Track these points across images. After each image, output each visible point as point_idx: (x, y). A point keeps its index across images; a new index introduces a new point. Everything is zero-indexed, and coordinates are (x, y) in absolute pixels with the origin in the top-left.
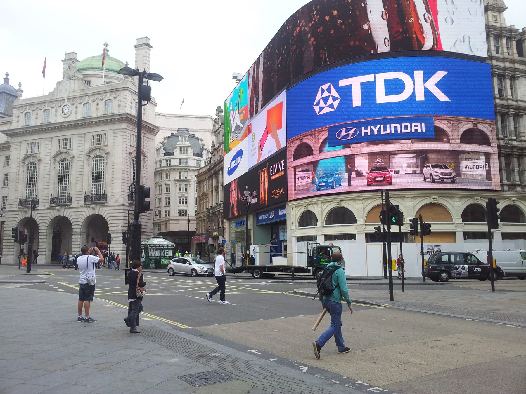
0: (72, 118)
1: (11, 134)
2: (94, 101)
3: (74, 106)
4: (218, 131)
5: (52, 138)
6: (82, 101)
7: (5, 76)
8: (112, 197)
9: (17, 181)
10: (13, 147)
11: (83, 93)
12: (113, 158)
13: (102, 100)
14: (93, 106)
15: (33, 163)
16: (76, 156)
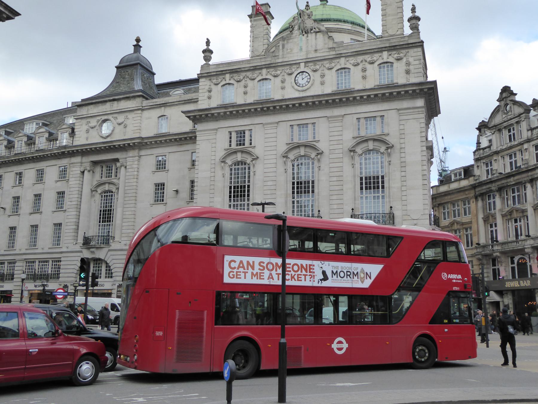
0: (316, 90)
1: (197, 117)
2: (357, 65)
3: (318, 74)
4: (505, 124)
5: (278, 123)
6: (333, 65)
7: (135, 43)
8: (406, 217)
9: (212, 191)
10: (202, 138)
11: (334, 53)
12: (403, 155)
13: (372, 63)
14: (356, 73)
15: (243, 163)
16: (326, 152)
